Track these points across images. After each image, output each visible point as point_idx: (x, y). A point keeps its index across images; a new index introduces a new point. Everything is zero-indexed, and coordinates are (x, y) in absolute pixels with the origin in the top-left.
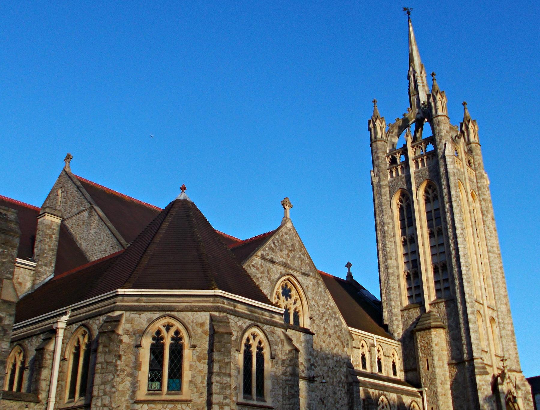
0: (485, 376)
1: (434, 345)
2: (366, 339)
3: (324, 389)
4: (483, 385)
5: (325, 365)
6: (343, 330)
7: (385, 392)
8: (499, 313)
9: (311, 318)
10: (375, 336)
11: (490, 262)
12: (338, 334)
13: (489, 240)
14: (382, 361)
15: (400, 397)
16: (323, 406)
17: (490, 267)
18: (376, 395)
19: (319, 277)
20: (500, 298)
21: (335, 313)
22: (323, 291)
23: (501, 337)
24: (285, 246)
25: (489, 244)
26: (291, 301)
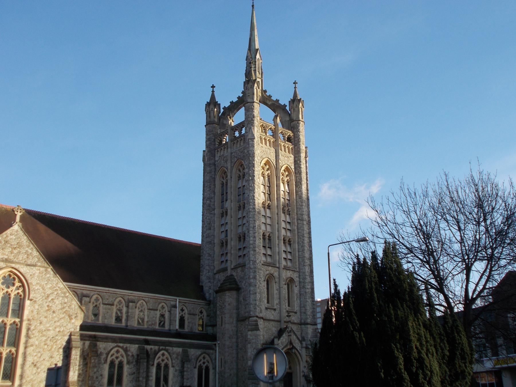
0: (255, 332)
1: (227, 304)
2: (167, 302)
3: (39, 355)
4: (253, 339)
5: (44, 336)
6: (73, 306)
7: (167, 348)
8: (301, 274)
10: (178, 299)
11: (298, 229)
12: (64, 310)
13: (300, 209)
14: (186, 318)
15: (187, 350)
16: (36, 368)
17: (298, 233)
18: (155, 351)
20: (303, 260)
22: (52, 276)
23: (300, 295)
24: (9, 245)
25: (299, 212)
26: (12, 288)
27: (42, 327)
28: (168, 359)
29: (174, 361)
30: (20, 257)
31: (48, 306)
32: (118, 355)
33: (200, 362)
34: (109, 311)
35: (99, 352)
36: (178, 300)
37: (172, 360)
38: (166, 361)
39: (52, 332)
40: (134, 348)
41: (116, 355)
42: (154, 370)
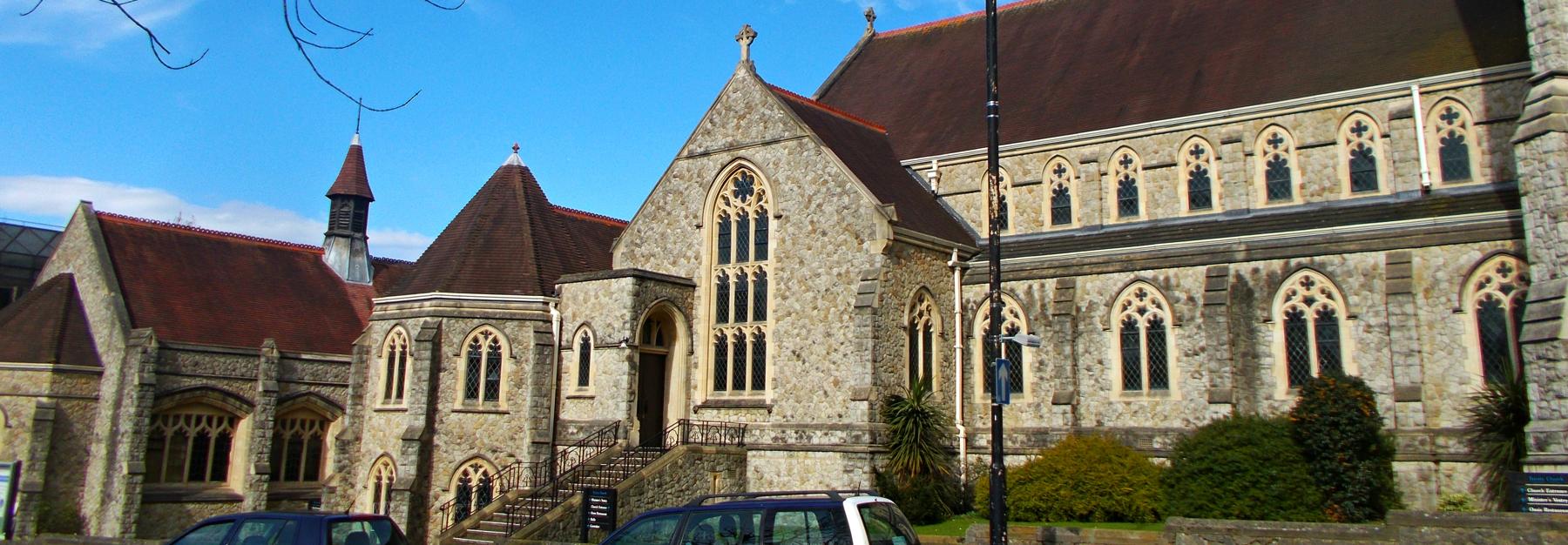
6: (862, 210)
9: (778, 217)
18: (1271, 275)
19: (799, 133)
21: (841, 185)
27: (805, 271)
28: (1330, 296)
29: (1353, 299)
30: (754, 131)
31: (812, 222)
32: (1141, 304)
33: (1481, 286)
34: (1164, 183)
35: (1084, 306)
36: (1415, 89)
37: (1345, 298)
38: (1322, 299)
39: (824, 278)
40: (1193, 279)
41: (1136, 303)
42: (1275, 339)
